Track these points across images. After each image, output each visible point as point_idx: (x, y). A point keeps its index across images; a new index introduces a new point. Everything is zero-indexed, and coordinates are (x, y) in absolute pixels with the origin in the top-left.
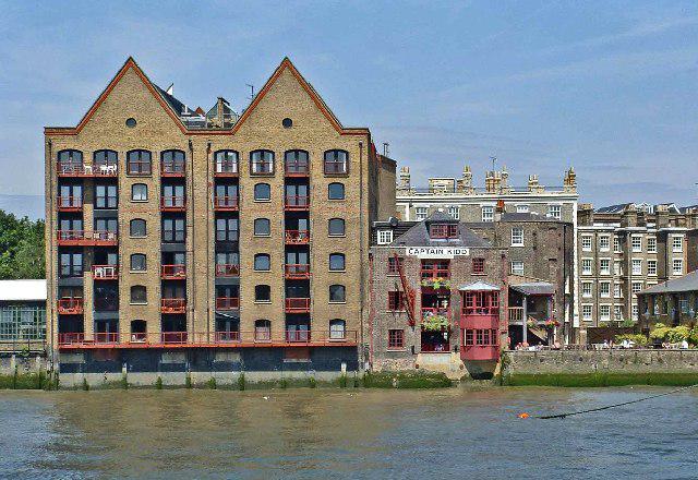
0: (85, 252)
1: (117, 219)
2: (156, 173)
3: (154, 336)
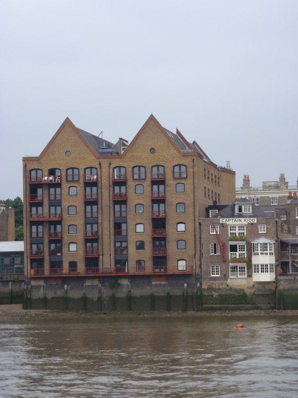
1: (61, 206)
2: (82, 180)
3: (81, 268)
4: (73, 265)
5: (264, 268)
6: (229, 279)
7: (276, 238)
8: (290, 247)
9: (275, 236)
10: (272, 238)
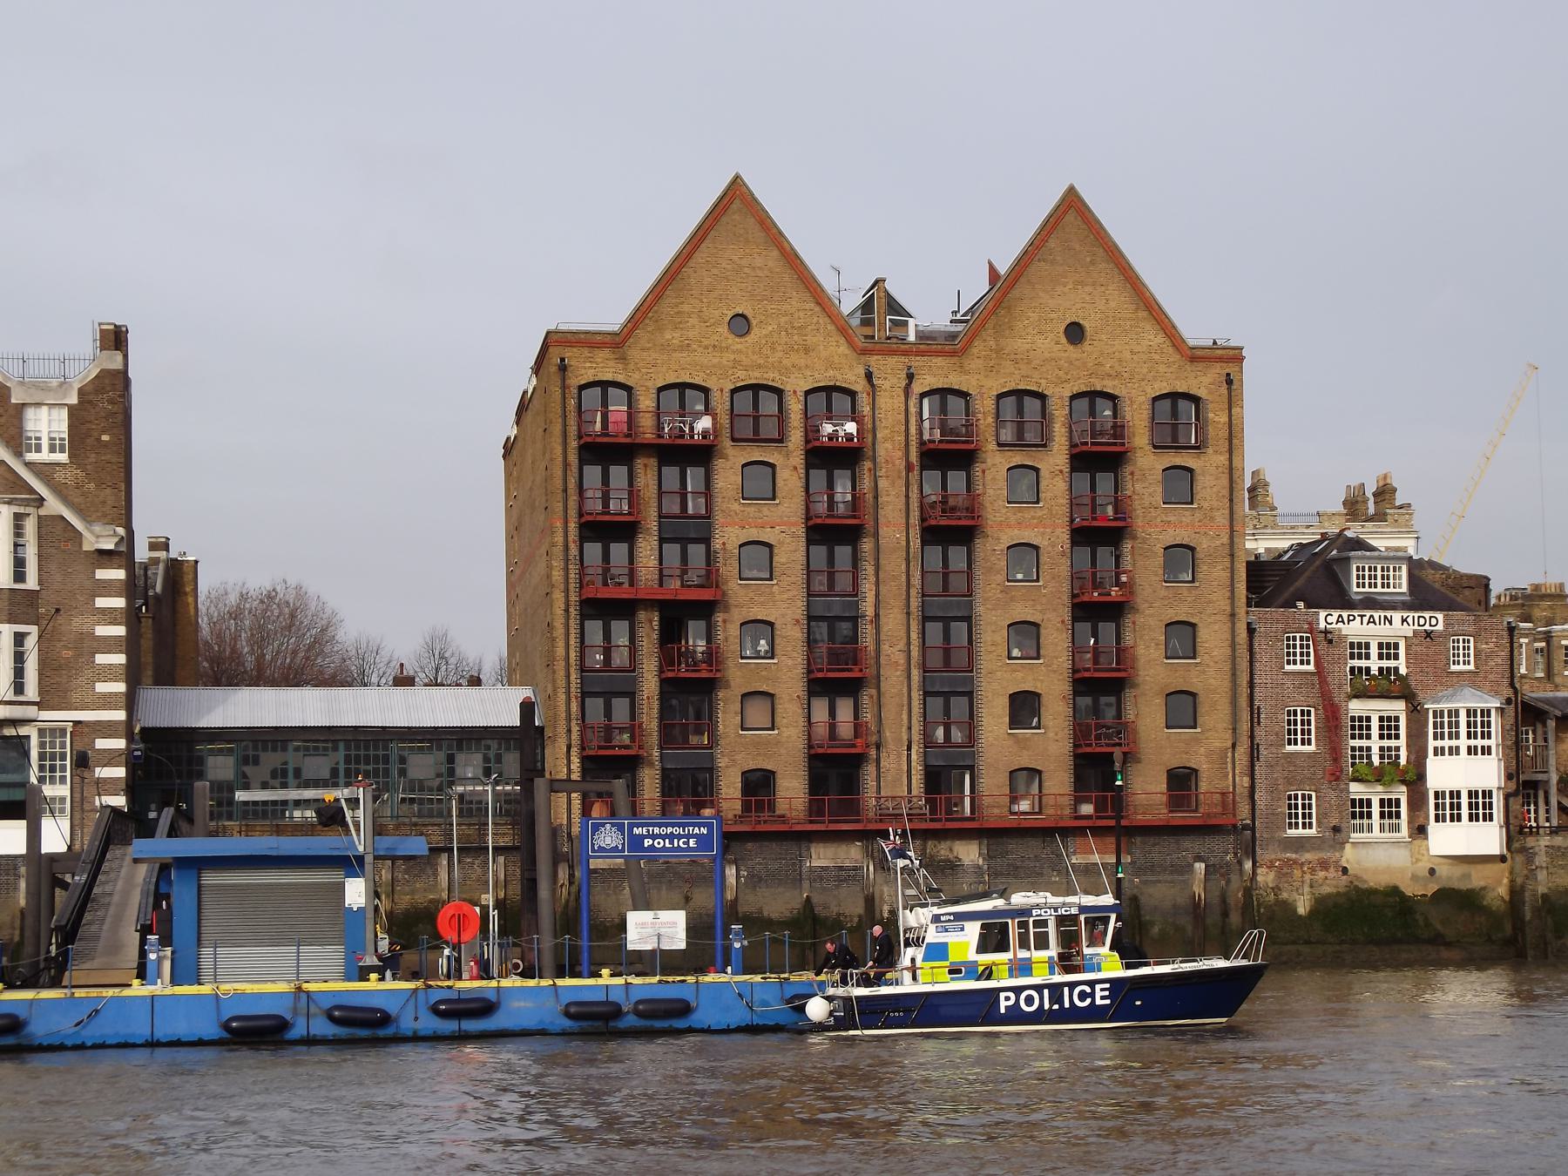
0: (642, 615)
1: (706, 540)
2: (796, 437)
4: (759, 784)
5: (1480, 805)
6: (1348, 846)
7: (1509, 692)
8: (1551, 724)
9: (1506, 682)
10: (1497, 693)
